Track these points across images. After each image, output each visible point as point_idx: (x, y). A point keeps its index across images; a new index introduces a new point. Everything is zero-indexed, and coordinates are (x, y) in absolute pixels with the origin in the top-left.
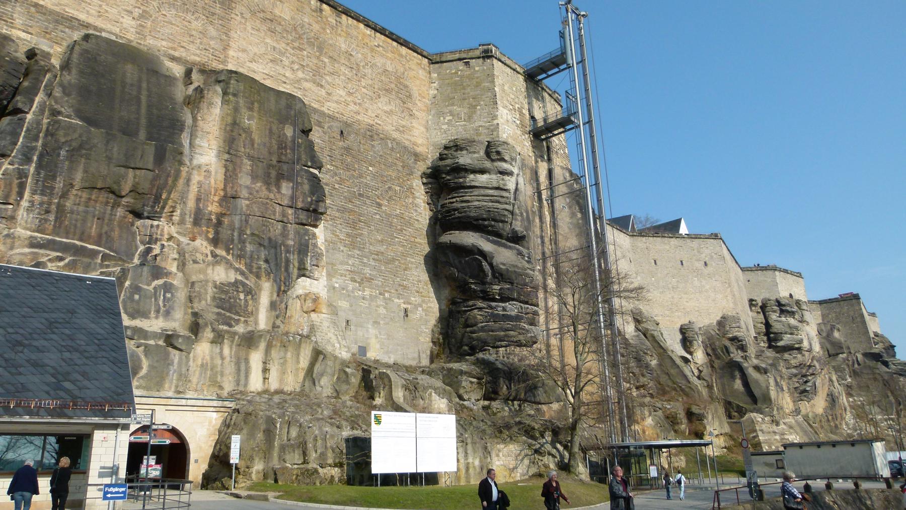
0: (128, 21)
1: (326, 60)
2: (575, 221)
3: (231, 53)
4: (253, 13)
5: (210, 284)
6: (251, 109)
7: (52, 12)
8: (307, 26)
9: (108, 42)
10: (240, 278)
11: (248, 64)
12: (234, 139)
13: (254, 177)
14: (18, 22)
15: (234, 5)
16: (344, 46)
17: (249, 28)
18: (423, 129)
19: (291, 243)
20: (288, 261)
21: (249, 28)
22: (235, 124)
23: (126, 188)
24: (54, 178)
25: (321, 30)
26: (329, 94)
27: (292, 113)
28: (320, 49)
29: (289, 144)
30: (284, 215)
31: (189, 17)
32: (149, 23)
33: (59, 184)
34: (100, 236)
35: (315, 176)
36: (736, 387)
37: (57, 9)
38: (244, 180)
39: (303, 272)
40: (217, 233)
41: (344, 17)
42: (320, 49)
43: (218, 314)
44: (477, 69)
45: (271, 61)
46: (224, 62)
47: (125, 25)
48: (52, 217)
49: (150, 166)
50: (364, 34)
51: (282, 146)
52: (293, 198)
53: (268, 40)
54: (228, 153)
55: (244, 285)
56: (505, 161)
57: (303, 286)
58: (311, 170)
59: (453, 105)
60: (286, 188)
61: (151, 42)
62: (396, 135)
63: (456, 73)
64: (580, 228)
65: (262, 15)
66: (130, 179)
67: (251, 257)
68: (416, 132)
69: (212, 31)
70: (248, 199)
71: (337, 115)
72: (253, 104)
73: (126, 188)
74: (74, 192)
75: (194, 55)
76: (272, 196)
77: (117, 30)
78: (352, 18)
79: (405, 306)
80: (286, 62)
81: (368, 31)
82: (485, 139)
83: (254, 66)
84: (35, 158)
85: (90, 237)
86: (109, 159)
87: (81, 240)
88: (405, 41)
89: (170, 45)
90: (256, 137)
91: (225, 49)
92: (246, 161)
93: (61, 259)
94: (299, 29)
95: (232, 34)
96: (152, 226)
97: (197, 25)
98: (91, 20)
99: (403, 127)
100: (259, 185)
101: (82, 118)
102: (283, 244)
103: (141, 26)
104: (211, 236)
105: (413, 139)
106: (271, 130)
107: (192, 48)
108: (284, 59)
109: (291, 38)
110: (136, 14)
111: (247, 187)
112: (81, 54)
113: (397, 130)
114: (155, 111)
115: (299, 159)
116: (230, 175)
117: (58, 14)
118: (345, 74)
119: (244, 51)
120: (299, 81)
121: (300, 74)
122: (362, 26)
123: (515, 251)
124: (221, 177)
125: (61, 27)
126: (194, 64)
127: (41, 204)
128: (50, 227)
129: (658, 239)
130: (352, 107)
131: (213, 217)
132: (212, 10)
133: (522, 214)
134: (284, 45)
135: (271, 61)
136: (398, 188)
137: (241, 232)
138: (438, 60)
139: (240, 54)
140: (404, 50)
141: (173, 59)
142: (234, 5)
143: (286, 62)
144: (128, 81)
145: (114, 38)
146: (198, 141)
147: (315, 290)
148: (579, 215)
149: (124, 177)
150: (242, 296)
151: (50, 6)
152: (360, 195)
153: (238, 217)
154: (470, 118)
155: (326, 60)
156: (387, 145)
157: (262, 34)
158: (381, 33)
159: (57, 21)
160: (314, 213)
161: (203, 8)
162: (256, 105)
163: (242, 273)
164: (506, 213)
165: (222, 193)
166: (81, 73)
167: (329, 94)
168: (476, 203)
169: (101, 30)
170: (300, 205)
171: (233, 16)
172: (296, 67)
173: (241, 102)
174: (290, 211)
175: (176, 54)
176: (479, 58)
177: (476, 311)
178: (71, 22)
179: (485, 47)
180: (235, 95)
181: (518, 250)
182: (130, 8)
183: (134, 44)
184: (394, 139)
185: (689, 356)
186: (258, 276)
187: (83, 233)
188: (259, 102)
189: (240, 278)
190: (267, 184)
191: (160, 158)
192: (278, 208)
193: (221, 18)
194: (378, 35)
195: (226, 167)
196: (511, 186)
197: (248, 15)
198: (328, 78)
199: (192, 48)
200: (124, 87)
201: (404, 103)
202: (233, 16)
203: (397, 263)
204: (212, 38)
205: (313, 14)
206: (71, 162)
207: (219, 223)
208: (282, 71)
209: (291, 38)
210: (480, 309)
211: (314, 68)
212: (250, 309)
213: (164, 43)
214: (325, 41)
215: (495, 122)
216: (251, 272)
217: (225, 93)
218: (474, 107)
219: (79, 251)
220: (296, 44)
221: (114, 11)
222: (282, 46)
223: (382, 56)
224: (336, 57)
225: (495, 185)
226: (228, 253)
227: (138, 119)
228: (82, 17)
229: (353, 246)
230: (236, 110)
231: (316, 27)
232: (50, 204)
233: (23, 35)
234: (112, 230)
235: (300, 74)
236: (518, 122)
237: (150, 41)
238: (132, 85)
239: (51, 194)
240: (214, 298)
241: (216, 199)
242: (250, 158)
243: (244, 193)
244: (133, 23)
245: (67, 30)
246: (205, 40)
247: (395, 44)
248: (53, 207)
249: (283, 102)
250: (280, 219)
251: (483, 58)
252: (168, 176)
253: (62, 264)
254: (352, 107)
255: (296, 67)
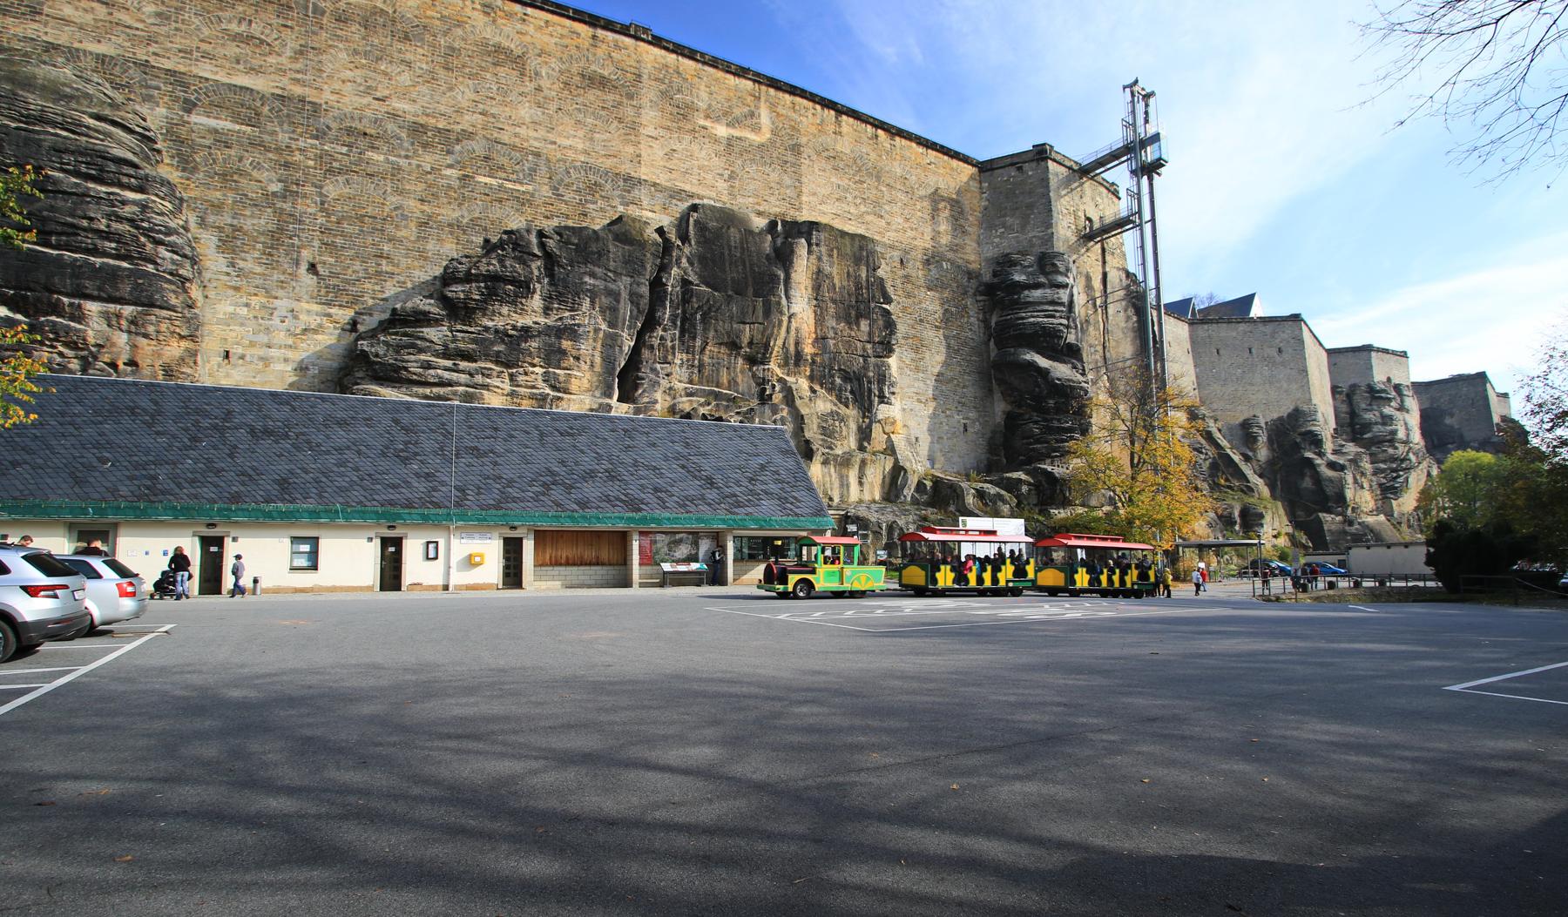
0: (722, 185)
1: (884, 189)
2: (1130, 325)
3: (804, 198)
4: (819, 154)
5: (815, 417)
6: (831, 256)
7: (666, 189)
8: (865, 156)
9: (712, 208)
10: (834, 408)
11: (819, 207)
12: (820, 286)
13: (838, 318)
14: (645, 203)
15: (802, 149)
16: (899, 171)
17: (816, 170)
18: (975, 245)
19: (871, 374)
20: (870, 390)
21: (816, 170)
22: (819, 271)
23: (745, 340)
24: (694, 338)
25: (878, 158)
26: (888, 224)
27: (865, 254)
28: (878, 178)
29: (864, 284)
30: (864, 349)
31: (767, 169)
32: (737, 182)
33: (698, 343)
34: (729, 382)
35: (888, 313)
36: (1304, 485)
37: (667, 184)
38: (831, 323)
39: (883, 399)
40: (812, 371)
41: (897, 139)
42: (878, 178)
43: (822, 440)
44: (1030, 173)
45: (837, 200)
46: (799, 209)
47: (719, 189)
48: (696, 371)
49: (760, 320)
50: (917, 153)
51: (858, 287)
52: (870, 334)
53: (833, 179)
54: (816, 299)
55: (838, 414)
56: (1061, 273)
57: (882, 411)
58: (884, 306)
59: (1005, 216)
60: (864, 325)
61: (741, 200)
62: (950, 255)
63: (1008, 180)
64: (1135, 332)
65: (826, 154)
66: (747, 333)
67: (840, 390)
68: (968, 249)
69: (787, 181)
70: (834, 338)
71: (897, 244)
72: (832, 251)
73: (745, 340)
74: (709, 348)
75: (775, 207)
76: (853, 334)
77: (714, 195)
78: (905, 138)
79: (965, 421)
80: (850, 198)
81: (921, 150)
82: (1038, 250)
83: (823, 208)
84: (679, 323)
85: (723, 384)
86: (731, 318)
87: (717, 387)
88: (956, 152)
89: (756, 200)
90: (836, 281)
91: (799, 196)
92: (830, 304)
93: (709, 404)
94: (858, 161)
95: (804, 180)
96: (764, 370)
97: (774, 176)
98: (694, 190)
99: (956, 246)
100: (842, 325)
101: (708, 285)
102: (865, 375)
103: (732, 187)
104: (808, 373)
105: (966, 257)
106: (848, 273)
107: (772, 199)
108: (848, 195)
109: (851, 172)
110: (726, 176)
111: (833, 328)
112: (695, 225)
113: (951, 250)
114: (756, 269)
115: (874, 297)
116: (820, 320)
117: (670, 189)
118: (901, 200)
119: (814, 194)
120: (862, 216)
121: (863, 208)
122: (914, 145)
123: (1070, 365)
124: (812, 321)
125: (674, 201)
126: (776, 216)
127: (688, 360)
128: (696, 378)
129: (1225, 325)
130: (910, 233)
131: (809, 357)
132: (785, 158)
133: (1076, 326)
134: (847, 181)
135: (837, 200)
136: (953, 309)
137: (832, 368)
138: (989, 167)
139: (811, 198)
140: (955, 163)
141: (760, 214)
142: (802, 149)
143: (850, 198)
144: (733, 244)
145: (712, 203)
146: (792, 292)
147: (892, 414)
148: (1135, 318)
149: (743, 331)
150: (837, 423)
151: (663, 183)
152: (921, 321)
153: (827, 355)
154: (1023, 227)
155: (884, 189)
156: (942, 267)
157: (828, 174)
158: (933, 149)
159: (671, 196)
160: (887, 348)
161: (778, 158)
162: (835, 251)
163: (836, 405)
164: (1062, 328)
165: (814, 336)
166: (698, 243)
167: (888, 224)
168: (1032, 320)
169: (701, 198)
170: (877, 339)
171: (802, 160)
172: (858, 201)
173: (823, 249)
174: (869, 346)
175: (761, 209)
176: (1032, 161)
177: (1031, 425)
178: (677, 194)
179: (1039, 148)
180: (817, 245)
181: (1073, 363)
182: (720, 172)
183: (728, 206)
184: (949, 260)
185: (1250, 454)
186: (847, 407)
187: (718, 382)
188: (837, 248)
189: (834, 408)
190: (849, 323)
191: (767, 313)
192: (859, 344)
193: (794, 165)
194: (930, 151)
195: (815, 312)
196: (1065, 299)
197: (814, 157)
198: (886, 207)
199: (772, 199)
200: (730, 250)
201: (957, 220)
202: (802, 160)
203: (955, 382)
204: (788, 187)
205: (871, 142)
206: (705, 324)
207: (814, 362)
208: (847, 209)
209: (851, 172)
210: (1036, 422)
211: (874, 199)
212: (844, 433)
213: (751, 200)
214: (882, 169)
215: (1049, 231)
216: (841, 403)
217: (810, 245)
218: (1029, 216)
219: (717, 396)
220: (857, 178)
221: (709, 177)
222: (844, 182)
223: (935, 173)
224: (892, 183)
225: (1050, 298)
226: (822, 388)
227: (746, 278)
228: (687, 188)
229: (917, 369)
230: (819, 259)
231: (873, 156)
232: (694, 360)
233: (650, 214)
234: (737, 376)
235: (863, 208)
236: (1073, 227)
237: (740, 200)
238: (735, 247)
239: (693, 355)
240: (819, 427)
241: (810, 341)
242: (834, 301)
243: (831, 334)
244: (725, 185)
245: (679, 203)
246: (782, 190)
247: (946, 158)
248: (696, 362)
249: (857, 243)
250: (861, 353)
251: (1038, 160)
252: (774, 327)
253: (709, 407)
254: (910, 233)
255: (858, 201)
